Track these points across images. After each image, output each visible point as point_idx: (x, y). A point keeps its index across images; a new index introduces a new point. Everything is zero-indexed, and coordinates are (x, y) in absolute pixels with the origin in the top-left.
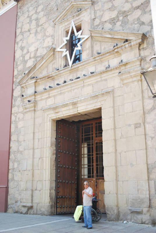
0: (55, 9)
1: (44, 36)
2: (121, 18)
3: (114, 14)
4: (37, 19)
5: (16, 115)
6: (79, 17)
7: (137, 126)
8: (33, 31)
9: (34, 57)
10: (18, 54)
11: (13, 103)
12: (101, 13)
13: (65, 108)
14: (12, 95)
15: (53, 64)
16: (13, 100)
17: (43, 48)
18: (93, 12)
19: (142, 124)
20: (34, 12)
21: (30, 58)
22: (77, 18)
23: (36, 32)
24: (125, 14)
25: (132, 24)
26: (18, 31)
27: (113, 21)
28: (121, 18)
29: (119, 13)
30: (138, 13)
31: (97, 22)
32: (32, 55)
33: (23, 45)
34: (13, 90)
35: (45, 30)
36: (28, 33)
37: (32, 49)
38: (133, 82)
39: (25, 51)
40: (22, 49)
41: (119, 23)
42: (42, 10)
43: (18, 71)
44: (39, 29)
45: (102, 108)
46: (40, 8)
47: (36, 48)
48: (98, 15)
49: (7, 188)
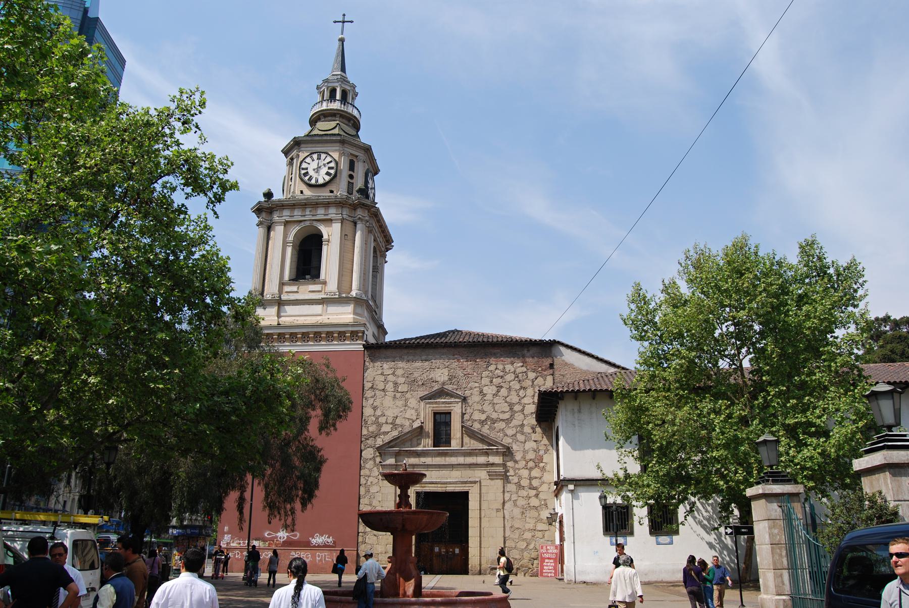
0: (420, 383)
1: (406, 406)
2: (489, 423)
3: (483, 417)
4: (396, 384)
5: (367, 478)
6: (450, 405)
7: (498, 510)
8: (390, 394)
9: (391, 424)
10: (368, 411)
11: (363, 465)
12: (472, 411)
13: (433, 485)
14: (361, 456)
15: (417, 440)
16: (362, 462)
17: (404, 418)
18: (464, 406)
19: (502, 510)
20: (390, 372)
21: (387, 423)
22: (447, 405)
23: (395, 397)
24: (494, 421)
25: (498, 432)
26: (368, 385)
27: (483, 423)
28: (489, 423)
29: (488, 417)
30: (502, 425)
31: (466, 417)
32: (390, 421)
33: (375, 404)
34: (361, 451)
35: (406, 400)
36: (383, 393)
37: (390, 414)
38: (497, 479)
39: (378, 413)
40: (375, 408)
41: (487, 427)
42: (403, 376)
43: (368, 431)
44: (398, 395)
45: (470, 492)
46: (399, 372)
47: (395, 415)
48: (468, 411)
49: (357, 550)
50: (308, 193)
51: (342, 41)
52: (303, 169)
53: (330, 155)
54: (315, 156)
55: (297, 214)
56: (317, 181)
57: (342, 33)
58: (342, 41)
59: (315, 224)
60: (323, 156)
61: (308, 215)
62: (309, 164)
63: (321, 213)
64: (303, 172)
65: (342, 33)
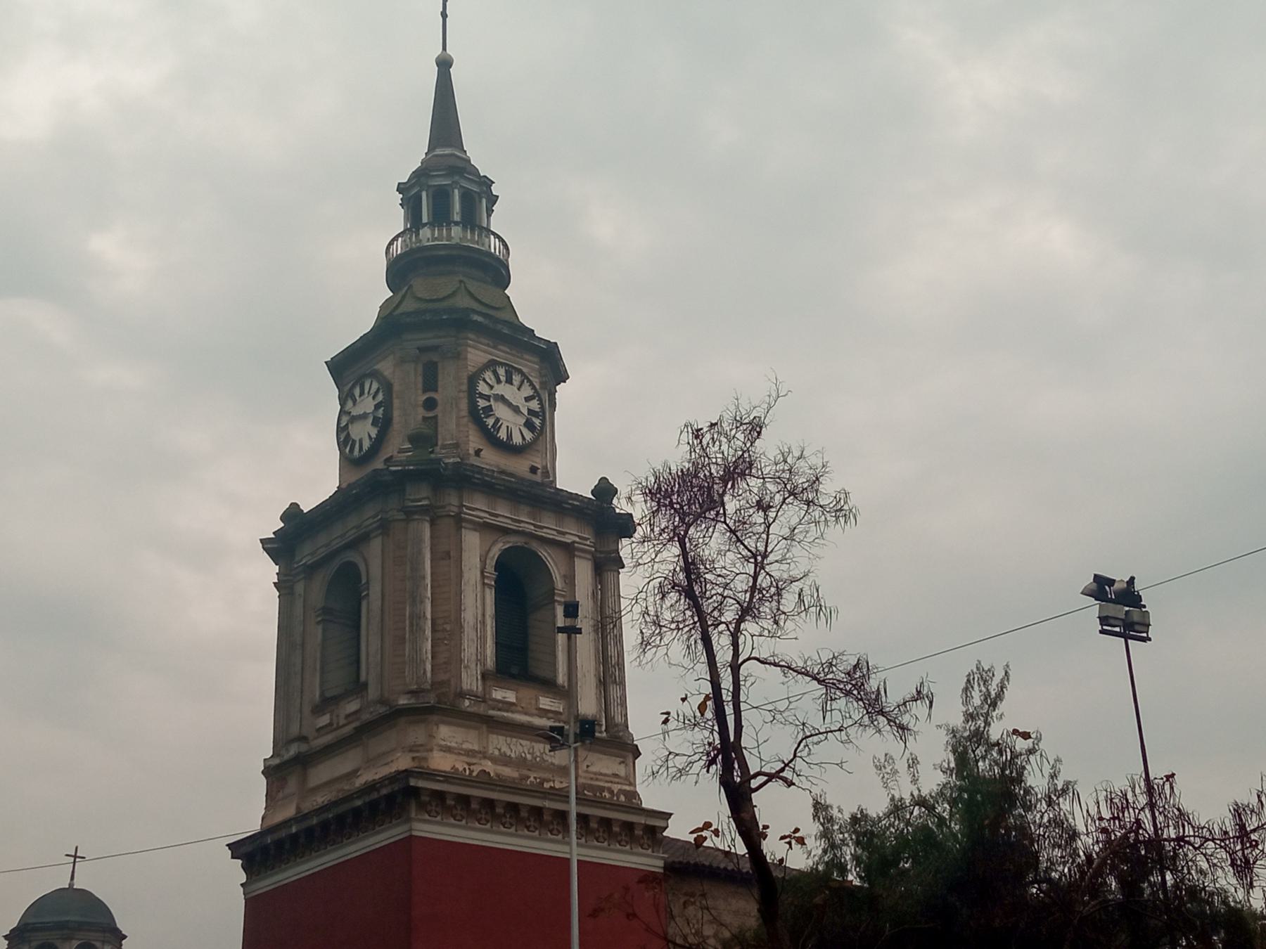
50: (491, 459)
51: (444, 65)
52: (482, 396)
53: (529, 381)
54: (501, 371)
55: (504, 513)
56: (510, 436)
57: (444, 48)
58: (444, 65)
59: (534, 546)
60: (516, 379)
61: (525, 520)
62: (491, 387)
63: (549, 526)
64: (482, 403)
65: (444, 48)
